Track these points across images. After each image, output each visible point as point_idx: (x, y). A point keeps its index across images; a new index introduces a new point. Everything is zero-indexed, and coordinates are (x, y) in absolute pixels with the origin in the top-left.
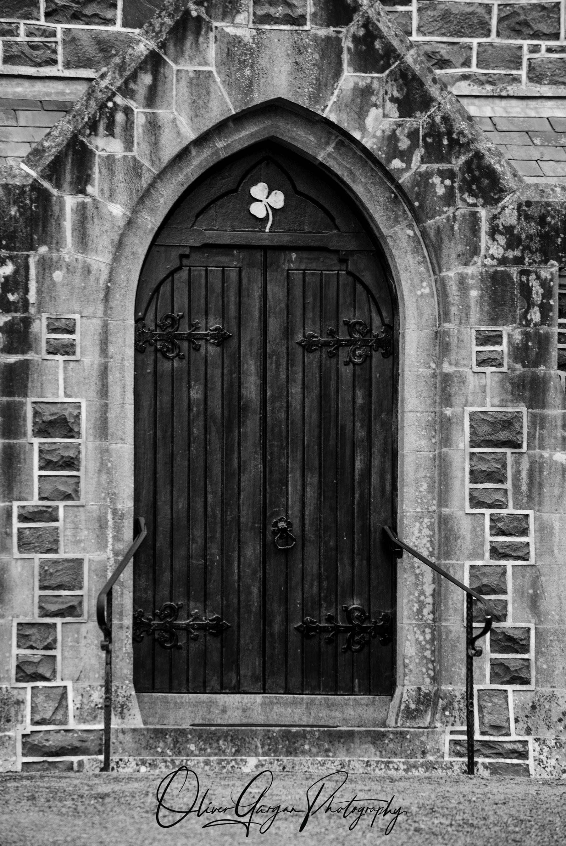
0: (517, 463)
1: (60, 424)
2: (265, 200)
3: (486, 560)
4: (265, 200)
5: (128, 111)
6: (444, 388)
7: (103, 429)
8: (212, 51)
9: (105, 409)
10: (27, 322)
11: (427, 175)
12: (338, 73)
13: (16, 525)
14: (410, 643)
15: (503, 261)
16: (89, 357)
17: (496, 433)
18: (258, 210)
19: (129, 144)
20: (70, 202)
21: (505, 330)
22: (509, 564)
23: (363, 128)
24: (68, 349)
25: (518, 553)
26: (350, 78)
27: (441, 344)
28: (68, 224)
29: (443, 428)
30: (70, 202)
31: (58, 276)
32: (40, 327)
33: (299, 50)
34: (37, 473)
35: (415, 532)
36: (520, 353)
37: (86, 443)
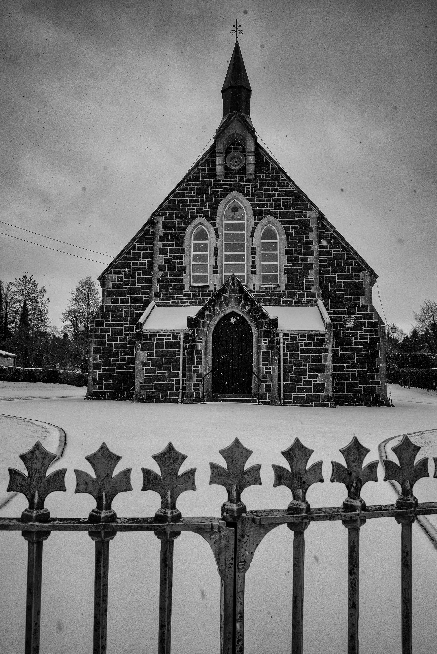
0: (269, 359)
1: (199, 353)
2: (233, 320)
3: (264, 374)
4: (233, 320)
5: (210, 308)
6: (259, 348)
7: (205, 354)
8: (222, 299)
9: (206, 351)
10: (195, 338)
11: (256, 315)
12: (242, 301)
13: (193, 368)
14: (254, 386)
15: (267, 328)
16: (204, 343)
17: (266, 354)
18: (232, 321)
19: (210, 313)
20: (201, 321)
21: (267, 339)
22: (268, 374)
23: (245, 309)
24: (201, 342)
25: (270, 372)
26: (243, 302)
27: (258, 341)
28: (201, 324)
29: (258, 354)
30: (201, 321)
31: (199, 332)
32: (197, 339)
33: (235, 298)
34: (196, 361)
35: (255, 370)
36: (269, 342)
37: (203, 357)
